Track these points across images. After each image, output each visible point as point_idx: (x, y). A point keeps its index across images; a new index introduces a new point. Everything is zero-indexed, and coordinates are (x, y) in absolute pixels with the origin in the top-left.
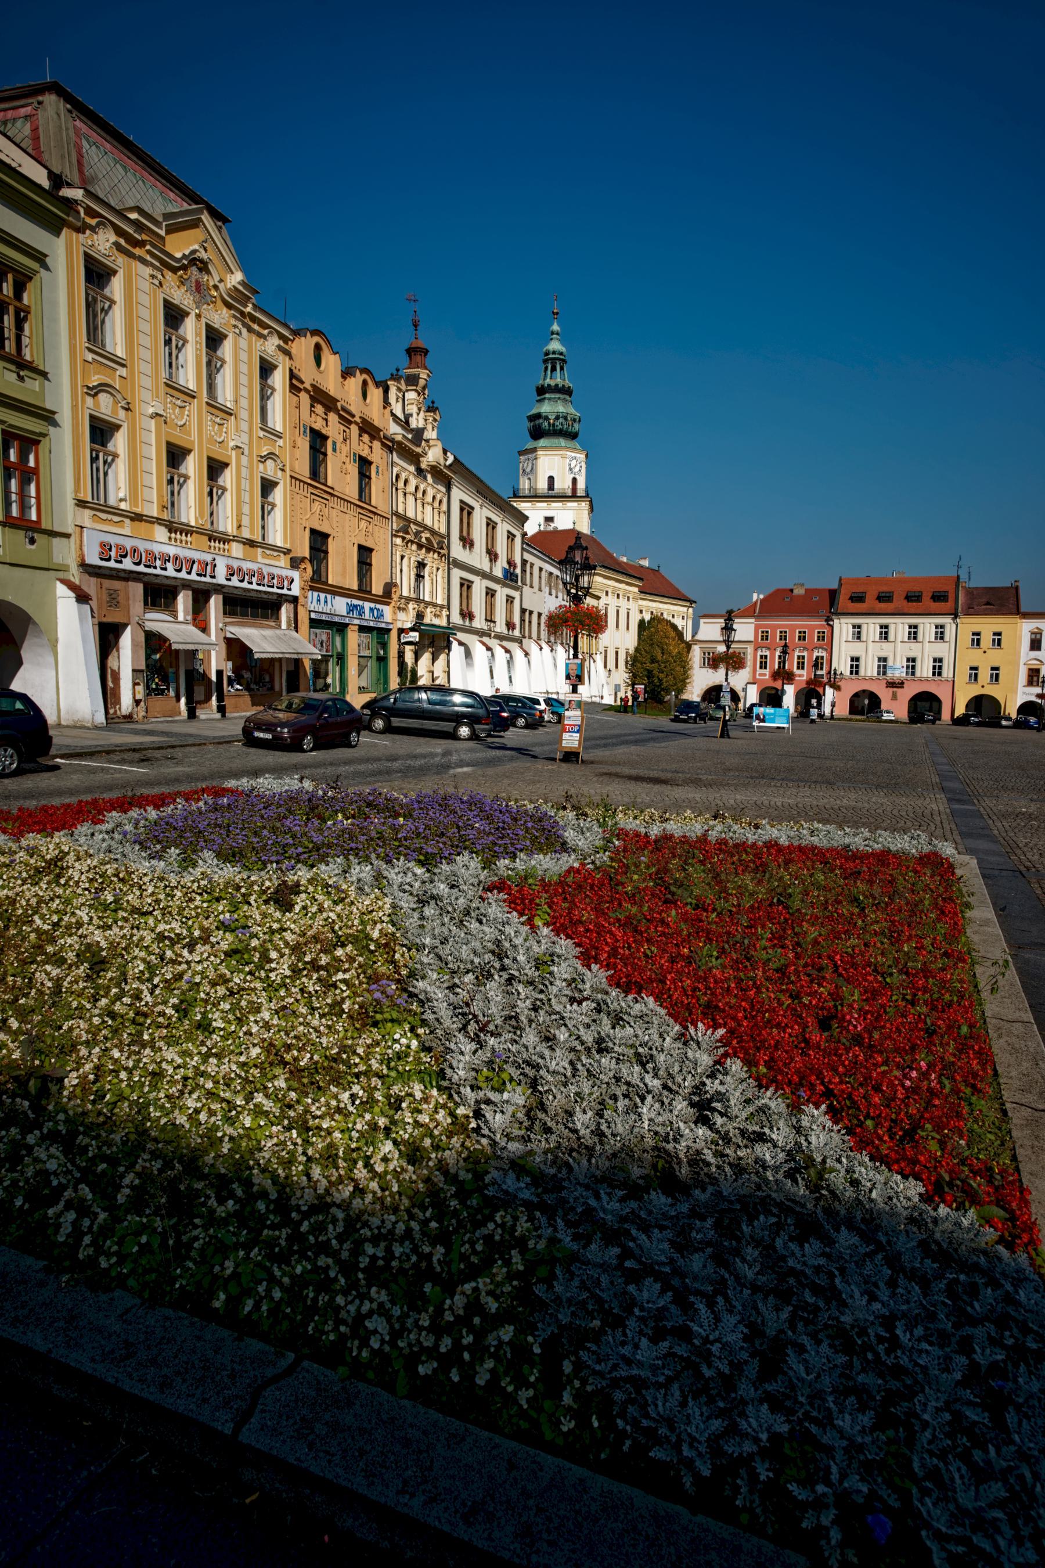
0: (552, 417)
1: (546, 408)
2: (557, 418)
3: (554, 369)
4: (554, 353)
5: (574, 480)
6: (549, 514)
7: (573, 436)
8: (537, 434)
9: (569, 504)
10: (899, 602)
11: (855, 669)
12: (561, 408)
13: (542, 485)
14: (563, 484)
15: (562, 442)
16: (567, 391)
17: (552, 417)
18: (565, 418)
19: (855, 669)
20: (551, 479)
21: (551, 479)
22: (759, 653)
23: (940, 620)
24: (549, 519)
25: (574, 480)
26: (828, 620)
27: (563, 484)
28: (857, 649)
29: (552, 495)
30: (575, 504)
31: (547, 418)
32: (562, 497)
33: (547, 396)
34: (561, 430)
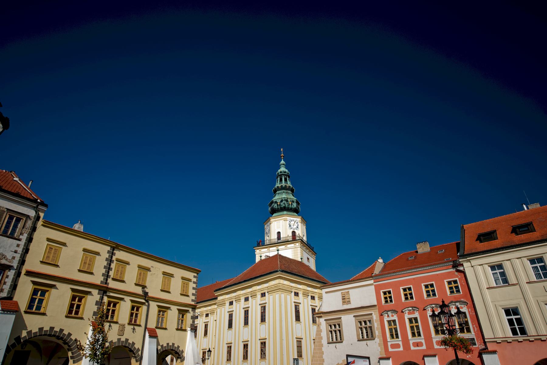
0: (279, 201)
1: (277, 198)
2: (282, 201)
3: (281, 180)
4: (281, 172)
5: (294, 233)
7: (296, 211)
8: (274, 211)
11: (517, 326)
12: (284, 196)
13: (274, 237)
14: (286, 234)
15: (285, 212)
16: (292, 191)
17: (279, 201)
18: (287, 201)
20: (279, 233)
21: (279, 233)
22: (386, 319)
25: (294, 233)
27: (286, 234)
28: (510, 297)
29: (280, 241)
30: (293, 245)
31: (276, 202)
32: (286, 242)
33: (278, 192)
34: (285, 207)
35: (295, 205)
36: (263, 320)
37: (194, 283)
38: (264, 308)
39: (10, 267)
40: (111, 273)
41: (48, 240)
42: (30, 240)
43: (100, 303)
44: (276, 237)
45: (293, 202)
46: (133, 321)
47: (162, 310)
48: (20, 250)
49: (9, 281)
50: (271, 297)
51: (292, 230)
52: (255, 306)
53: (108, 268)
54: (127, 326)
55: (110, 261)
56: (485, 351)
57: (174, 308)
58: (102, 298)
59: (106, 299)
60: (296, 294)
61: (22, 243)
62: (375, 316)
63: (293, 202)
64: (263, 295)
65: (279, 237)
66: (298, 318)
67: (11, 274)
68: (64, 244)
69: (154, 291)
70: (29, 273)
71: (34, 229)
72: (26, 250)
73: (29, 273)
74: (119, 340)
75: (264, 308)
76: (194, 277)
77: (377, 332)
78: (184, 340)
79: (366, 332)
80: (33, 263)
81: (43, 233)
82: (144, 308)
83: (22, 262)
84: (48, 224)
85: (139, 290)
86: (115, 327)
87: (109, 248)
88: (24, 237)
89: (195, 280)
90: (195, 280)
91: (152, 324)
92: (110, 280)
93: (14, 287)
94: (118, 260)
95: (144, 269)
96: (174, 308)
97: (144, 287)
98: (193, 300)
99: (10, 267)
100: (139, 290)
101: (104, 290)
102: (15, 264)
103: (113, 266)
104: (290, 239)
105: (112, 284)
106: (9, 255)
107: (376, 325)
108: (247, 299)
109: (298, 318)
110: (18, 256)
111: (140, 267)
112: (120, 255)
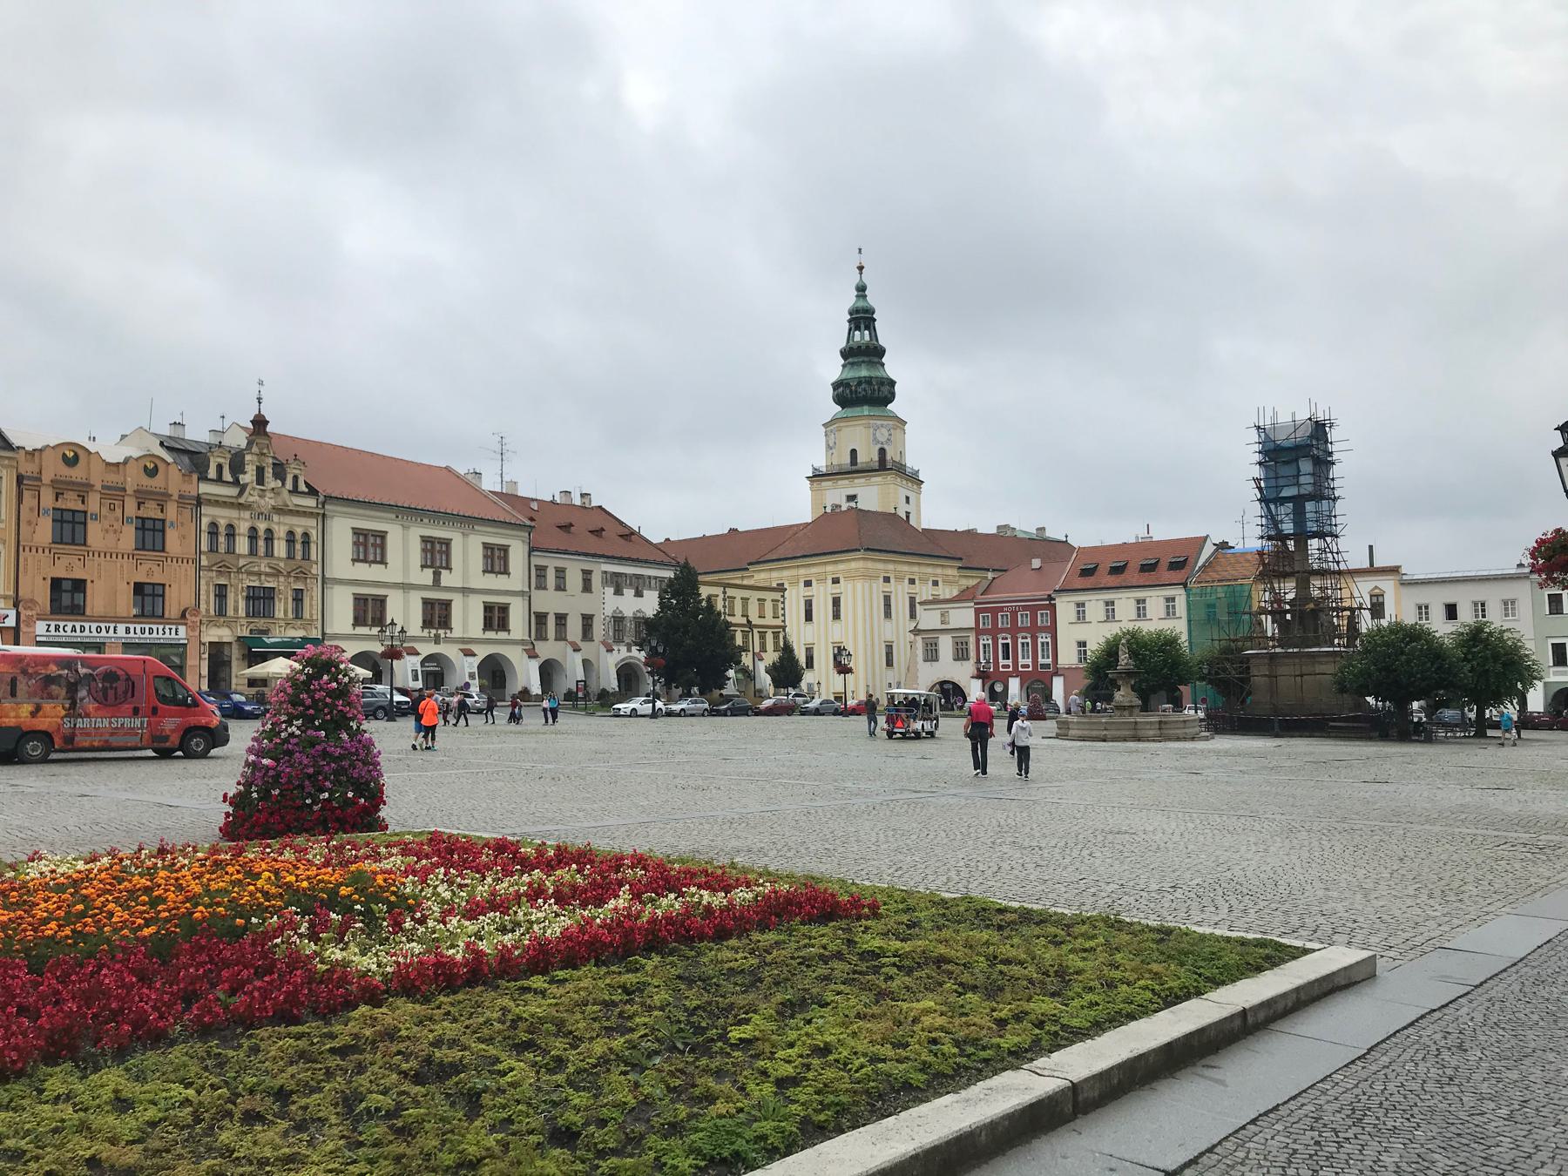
2: (860, 383)
5: (882, 452)
6: (851, 492)
10: (1132, 575)
14: (868, 456)
15: (866, 410)
20: (854, 452)
21: (854, 452)
23: (1170, 592)
24: (852, 498)
25: (882, 452)
26: (1050, 598)
28: (1081, 632)
32: (867, 471)
36: (837, 616)
38: (836, 602)
44: (848, 460)
45: (882, 384)
47: (762, 636)
50: (850, 586)
52: (822, 597)
56: (1056, 674)
57: (770, 631)
60: (887, 580)
62: (972, 640)
63: (882, 384)
64: (836, 581)
66: (888, 614)
69: (755, 620)
75: (836, 602)
77: (972, 654)
79: (961, 654)
85: (744, 621)
91: (757, 650)
95: (745, 600)
96: (770, 631)
104: (876, 466)
107: (972, 647)
108: (808, 584)
109: (888, 614)
112: (730, 592)
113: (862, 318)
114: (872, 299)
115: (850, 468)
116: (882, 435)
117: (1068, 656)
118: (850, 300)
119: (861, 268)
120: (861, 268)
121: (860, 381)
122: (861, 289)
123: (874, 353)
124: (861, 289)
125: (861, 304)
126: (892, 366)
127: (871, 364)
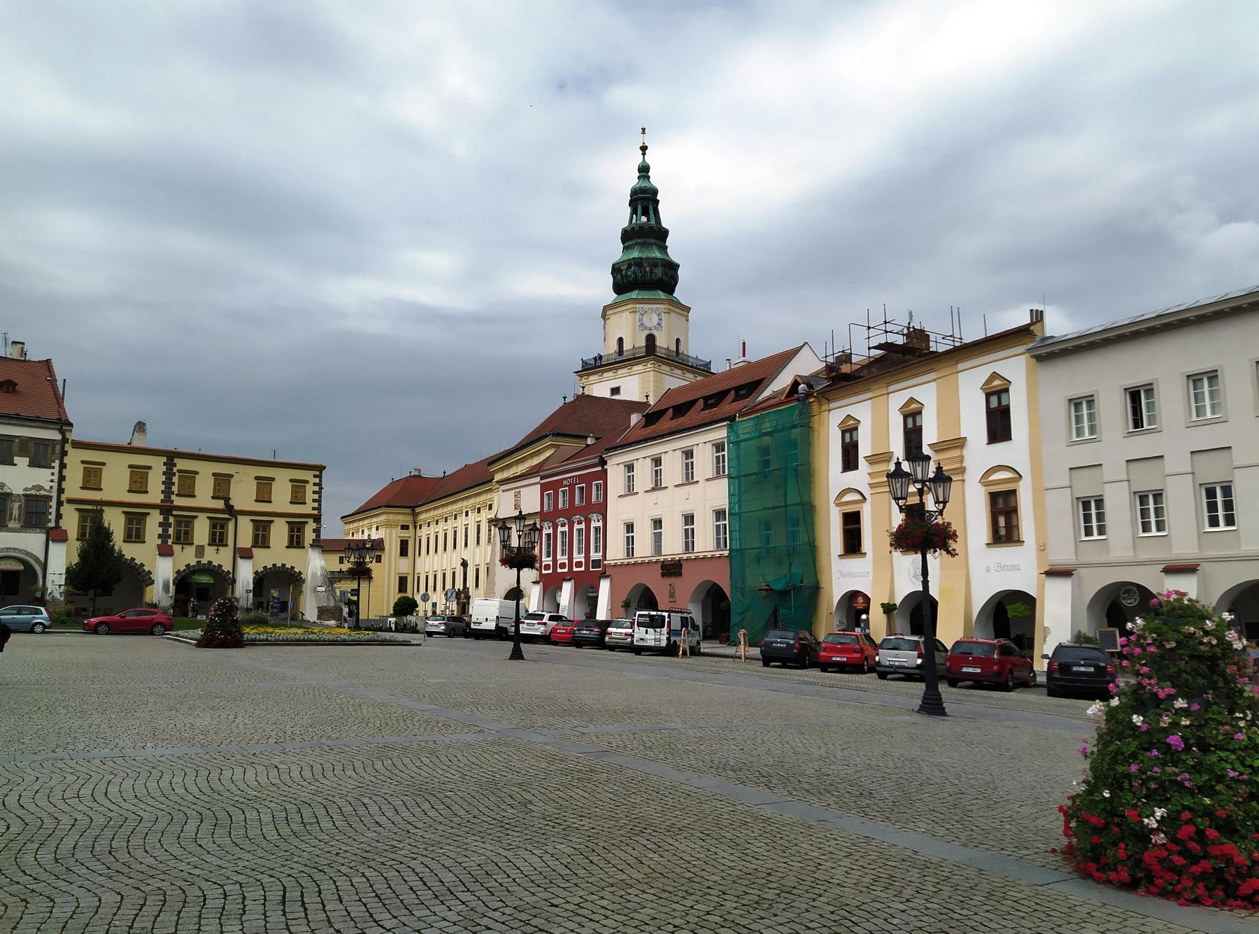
2: (629, 267)
5: (651, 339)
6: (614, 384)
9: (635, 368)
19: (630, 551)
20: (621, 340)
21: (621, 340)
24: (615, 391)
25: (651, 339)
26: (603, 462)
30: (640, 367)
32: (634, 360)
34: (636, 279)
35: (659, 271)
37: (315, 484)
39: (50, 498)
40: (175, 489)
41: (83, 462)
42: (63, 466)
43: (164, 525)
46: (217, 539)
48: (56, 478)
49: (53, 510)
51: (647, 332)
53: (168, 483)
54: (207, 548)
55: (169, 474)
56: (604, 575)
58: (166, 519)
59: (171, 520)
61: (56, 471)
65: (621, 351)
67: (53, 503)
68: (104, 464)
70: (70, 501)
71: (64, 453)
72: (62, 478)
73: (70, 501)
74: (199, 562)
76: (315, 476)
78: (306, 562)
80: (73, 489)
81: (74, 458)
82: (231, 525)
83: (61, 491)
84: (78, 445)
85: (220, 504)
86: (190, 551)
87: (165, 459)
88: (56, 464)
89: (317, 480)
90: (317, 480)
92: (173, 497)
93: (59, 516)
94: (179, 471)
97: (227, 500)
98: (314, 509)
99: (50, 498)
100: (220, 504)
101: (166, 509)
102: (54, 494)
103: (175, 479)
105: (178, 501)
106: (47, 486)
110: (55, 485)
111: (214, 474)
112: (181, 464)
113: (644, 199)
114: (655, 179)
115: (615, 357)
116: (651, 320)
117: (616, 552)
118: (633, 180)
119: (644, 149)
120: (644, 149)
121: (638, 262)
122: (644, 170)
123: (660, 235)
124: (644, 170)
125: (644, 184)
126: (675, 249)
127: (645, 246)
